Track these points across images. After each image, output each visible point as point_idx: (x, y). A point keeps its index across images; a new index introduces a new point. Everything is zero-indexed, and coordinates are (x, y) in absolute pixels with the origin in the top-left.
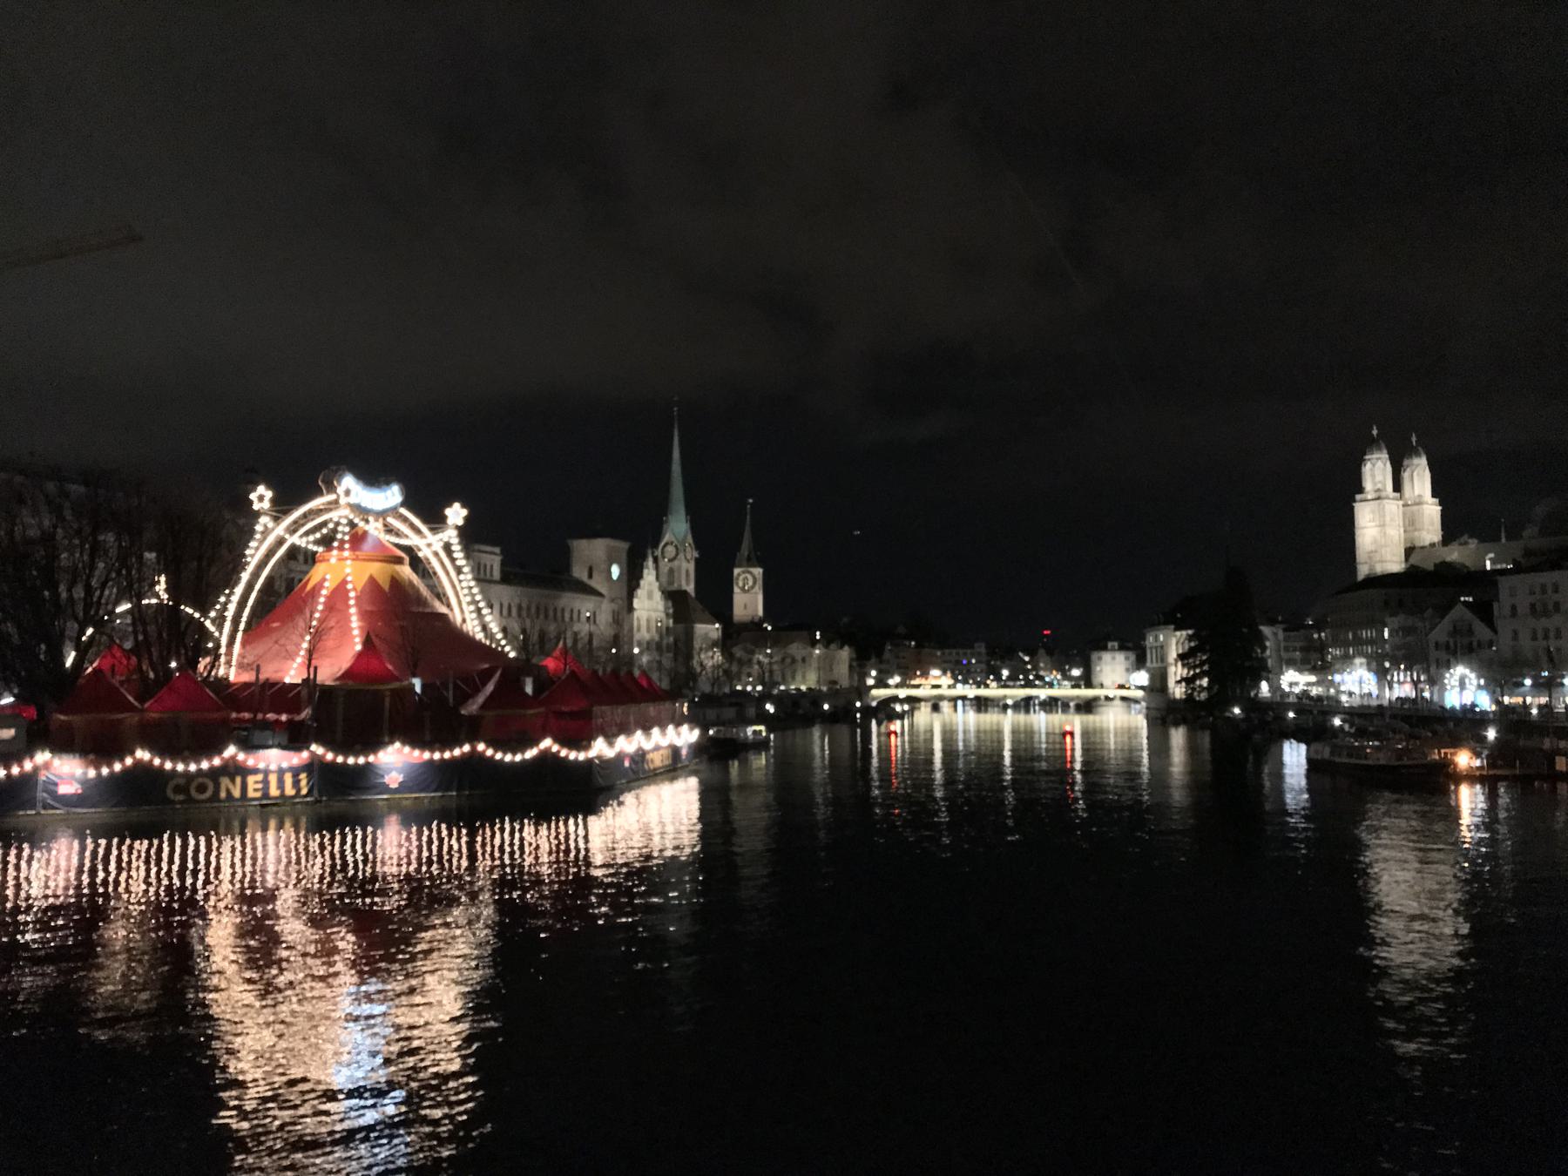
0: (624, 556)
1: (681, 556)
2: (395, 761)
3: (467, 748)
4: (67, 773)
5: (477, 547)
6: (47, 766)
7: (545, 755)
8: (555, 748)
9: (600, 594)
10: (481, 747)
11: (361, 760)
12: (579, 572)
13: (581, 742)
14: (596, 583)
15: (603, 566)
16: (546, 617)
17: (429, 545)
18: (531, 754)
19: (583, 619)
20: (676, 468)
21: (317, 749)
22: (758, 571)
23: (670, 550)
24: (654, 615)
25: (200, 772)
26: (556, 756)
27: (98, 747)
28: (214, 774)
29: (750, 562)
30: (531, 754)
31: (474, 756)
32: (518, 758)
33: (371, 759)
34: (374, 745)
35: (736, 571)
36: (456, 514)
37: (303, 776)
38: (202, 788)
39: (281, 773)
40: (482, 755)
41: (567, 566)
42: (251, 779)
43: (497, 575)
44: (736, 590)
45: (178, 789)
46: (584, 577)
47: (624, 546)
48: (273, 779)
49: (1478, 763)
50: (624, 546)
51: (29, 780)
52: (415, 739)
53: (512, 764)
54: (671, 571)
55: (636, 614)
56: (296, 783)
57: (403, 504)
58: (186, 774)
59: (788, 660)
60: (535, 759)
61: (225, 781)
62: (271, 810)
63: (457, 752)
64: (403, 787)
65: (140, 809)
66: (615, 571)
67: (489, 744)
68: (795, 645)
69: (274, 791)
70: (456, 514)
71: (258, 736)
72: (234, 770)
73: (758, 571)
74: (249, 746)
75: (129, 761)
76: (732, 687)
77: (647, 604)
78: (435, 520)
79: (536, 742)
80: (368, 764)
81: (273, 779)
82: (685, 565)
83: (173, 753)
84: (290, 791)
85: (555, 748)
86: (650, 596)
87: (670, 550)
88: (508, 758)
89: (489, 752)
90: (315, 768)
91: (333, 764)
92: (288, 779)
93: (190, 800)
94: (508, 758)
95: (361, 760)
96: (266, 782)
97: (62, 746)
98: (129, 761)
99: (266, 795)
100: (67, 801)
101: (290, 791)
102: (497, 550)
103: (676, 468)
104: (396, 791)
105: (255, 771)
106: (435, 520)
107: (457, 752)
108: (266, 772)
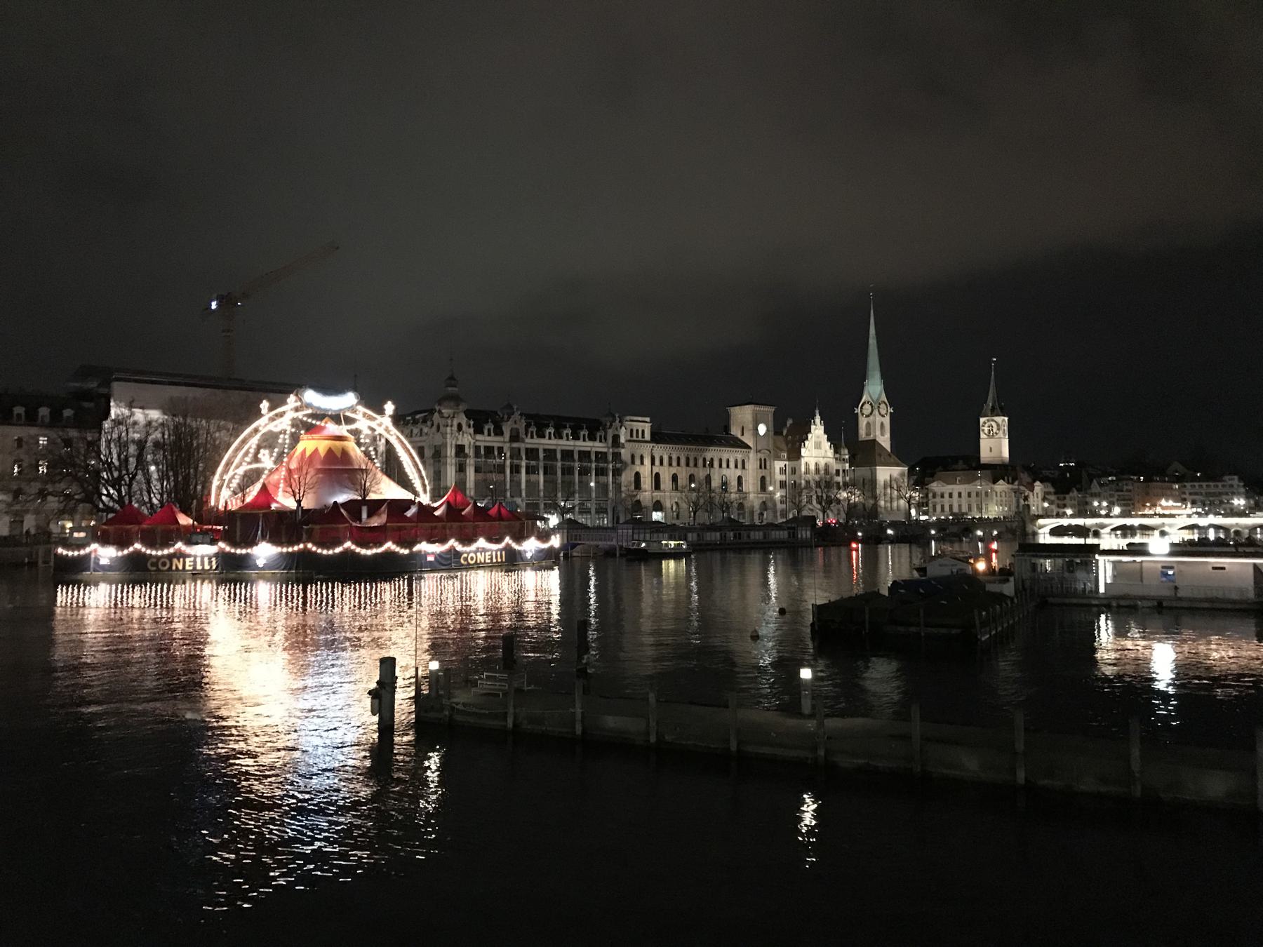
0: (770, 418)
1: (876, 412)
2: (264, 552)
3: (301, 546)
4: (106, 554)
5: (628, 418)
6: (95, 551)
7: (347, 552)
8: (353, 547)
9: (749, 447)
10: (310, 545)
11: (244, 551)
12: (735, 431)
13: (410, 544)
14: (748, 439)
15: (751, 426)
16: (696, 465)
17: (380, 425)
18: (338, 550)
19: (732, 465)
20: (872, 341)
21: (222, 545)
22: (1003, 420)
23: (867, 409)
24: (822, 462)
25: (163, 556)
26: (353, 552)
27: (121, 543)
28: (170, 557)
29: (994, 412)
30: (338, 550)
31: (306, 552)
32: (331, 552)
33: (249, 551)
34: (252, 543)
35: (982, 420)
36: (389, 407)
37: (214, 559)
38: (164, 564)
39: (202, 557)
40: (309, 551)
41: (727, 429)
42: (188, 560)
43: (648, 437)
44: (982, 435)
45: (153, 565)
46: (739, 436)
47: (770, 410)
48: (198, 560)
49: (1102, 590)
50: (770, 410)
51: (88, 556)
52: (275, 540)
53: (328, 556)
54: (868, 424)
55: (803, 461)
56: (210, 563)
57: (358, 404)
58: (158, 558)
59: (930, 495)
60: (341, 553)
61: (175, 561)
62: (197, 575)
63: (296, 548)
64: (265, 567)
65: (138, 572)
66: (762, 429)
67: (315, 544)
68: (934, 484)
69: (199, 567)
70: (389, 407)
71: (195, 538)
72: (181, 555)
73: (1003, 420)
74: (190, 543)
75: (131, 549)
76: (563, 512)
77: (815, 452)
78: (381, 412)
79: (340, 543)
80: (248, 555)
81: (198, 560)
82: (879, 419)
83: (323, 548)
84: (207, 567)
85: (353, 547)
86: (818, 446)
87: (867, 409)
88: (325, 552)
89: (314, 549)
90: (221, 556)
91: (229, 553)
92: (206, 560)
93: (158, 570)
94: (325, 552)
95: (244, 551)
96: (195, 562)
97: (105, 541)
98: (131, 549)
99: (195, 569)
100: (104, 568)
101: (207, 567)
102: (648, 419)
103: (872, 341)
104: (263, 569)
105: (189, 556)
106: (381, 412)
107: (296, 548)
108: (195, 557)
